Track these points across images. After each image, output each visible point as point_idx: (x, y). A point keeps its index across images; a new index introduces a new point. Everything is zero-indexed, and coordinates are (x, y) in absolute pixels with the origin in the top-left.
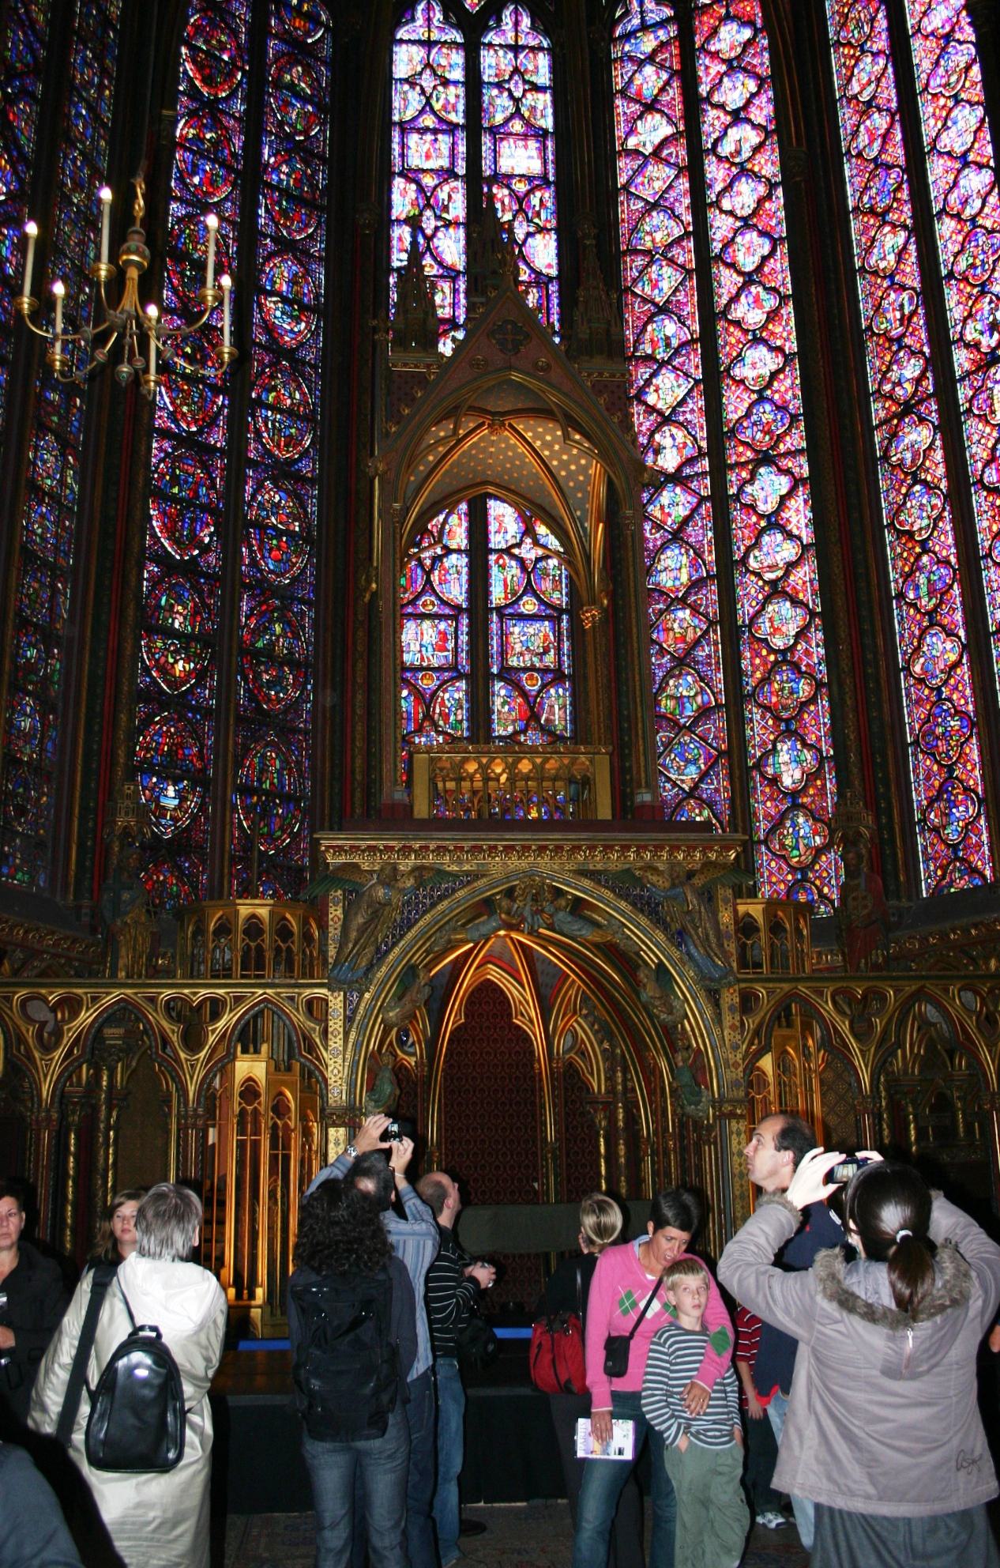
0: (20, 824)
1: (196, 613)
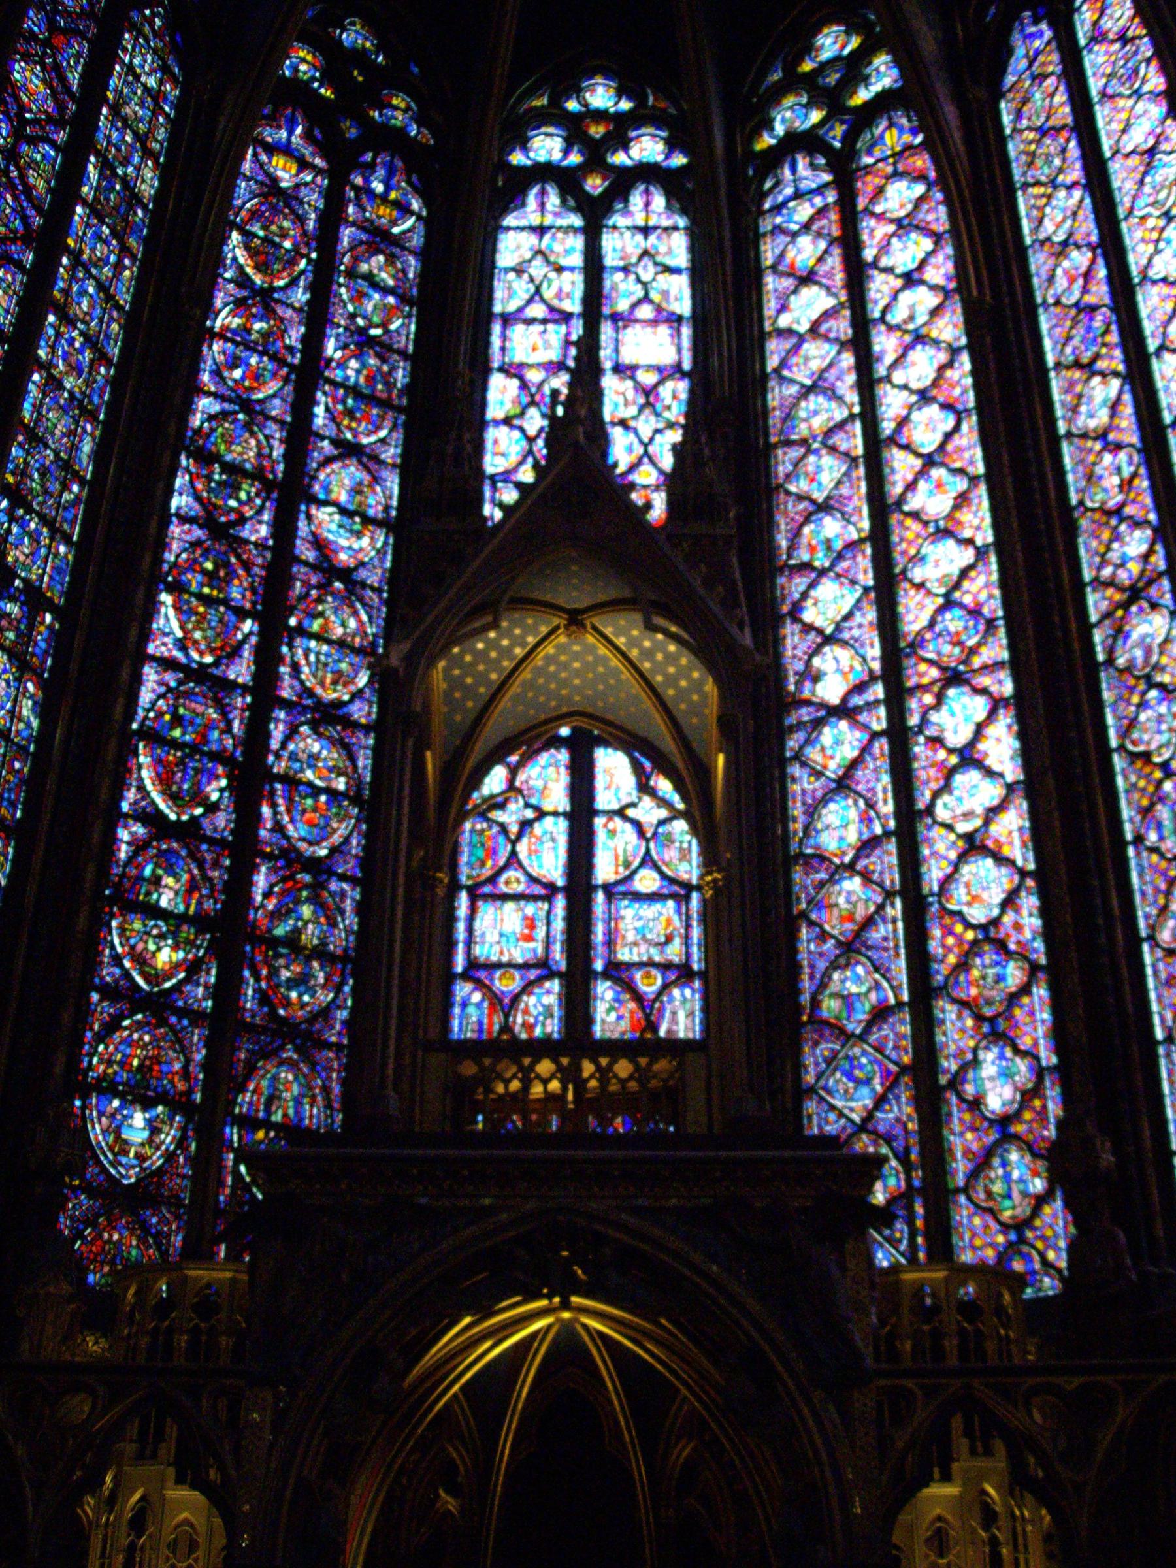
1: (192, 887)
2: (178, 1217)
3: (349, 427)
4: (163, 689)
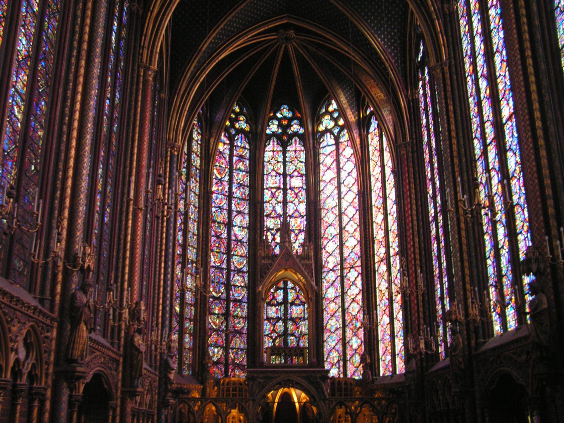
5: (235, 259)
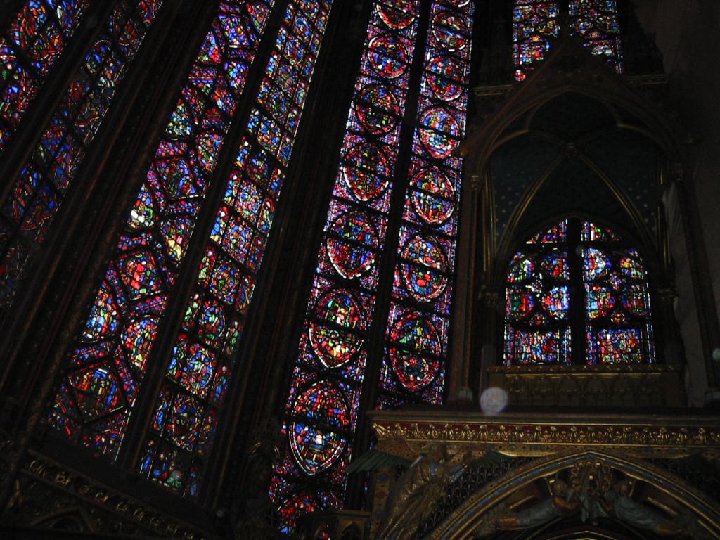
0: (179, 441)
2: (339, 498)
3: (439, 93)
4: (340, 213)
5: (418, 205)
